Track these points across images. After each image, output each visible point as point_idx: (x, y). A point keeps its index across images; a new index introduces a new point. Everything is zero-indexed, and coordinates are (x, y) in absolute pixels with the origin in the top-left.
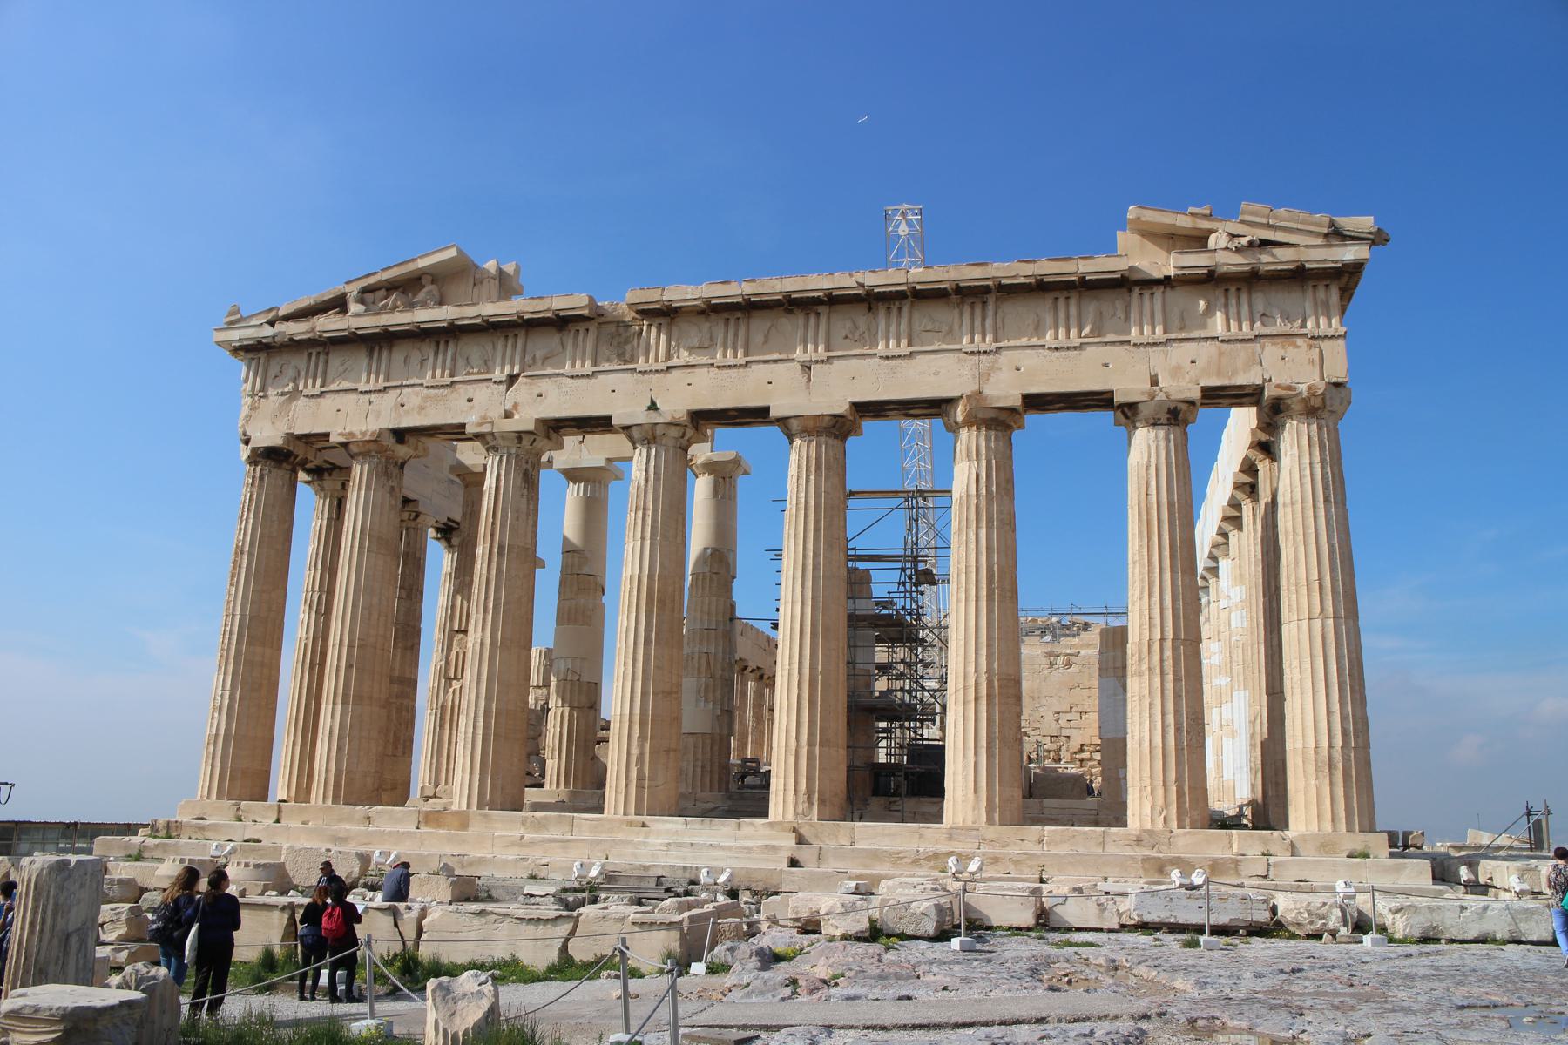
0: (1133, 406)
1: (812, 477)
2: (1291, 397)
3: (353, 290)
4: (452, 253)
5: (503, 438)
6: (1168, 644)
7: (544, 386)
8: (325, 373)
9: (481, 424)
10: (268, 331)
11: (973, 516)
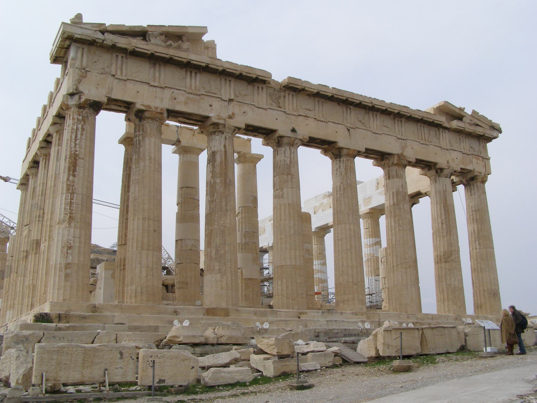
0: (442, 170)
5: (229, 128)
7: (246, 108)
9: (220, 119)
10: (100, 36)
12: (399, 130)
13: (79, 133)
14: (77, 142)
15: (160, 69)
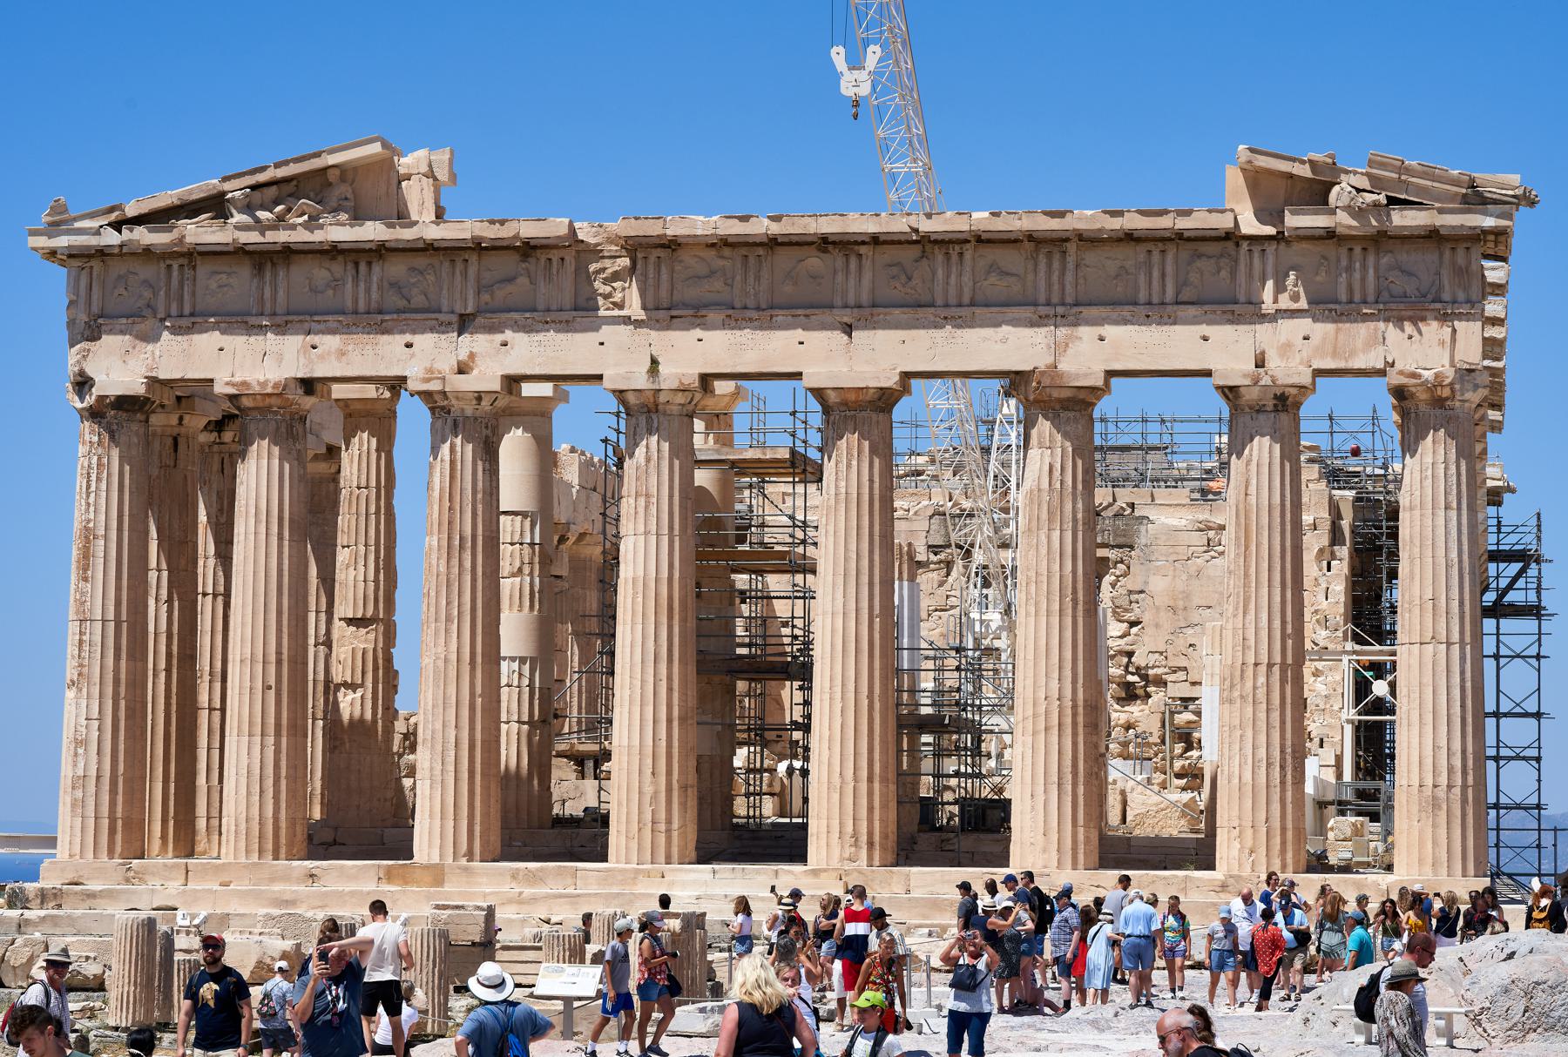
0: (1231, 388)
1: (855, 463)
2: (1415, 386)
3: (235, 190)
4: (375, 148)
5: (457, 398)
6: (1263, 669)
8: (194, 294)
9: (428, 380)
11: (1044, 515)
12: (1049, 285)
13: (94, 477)
14: (92, 500)
15: (275, 276)
